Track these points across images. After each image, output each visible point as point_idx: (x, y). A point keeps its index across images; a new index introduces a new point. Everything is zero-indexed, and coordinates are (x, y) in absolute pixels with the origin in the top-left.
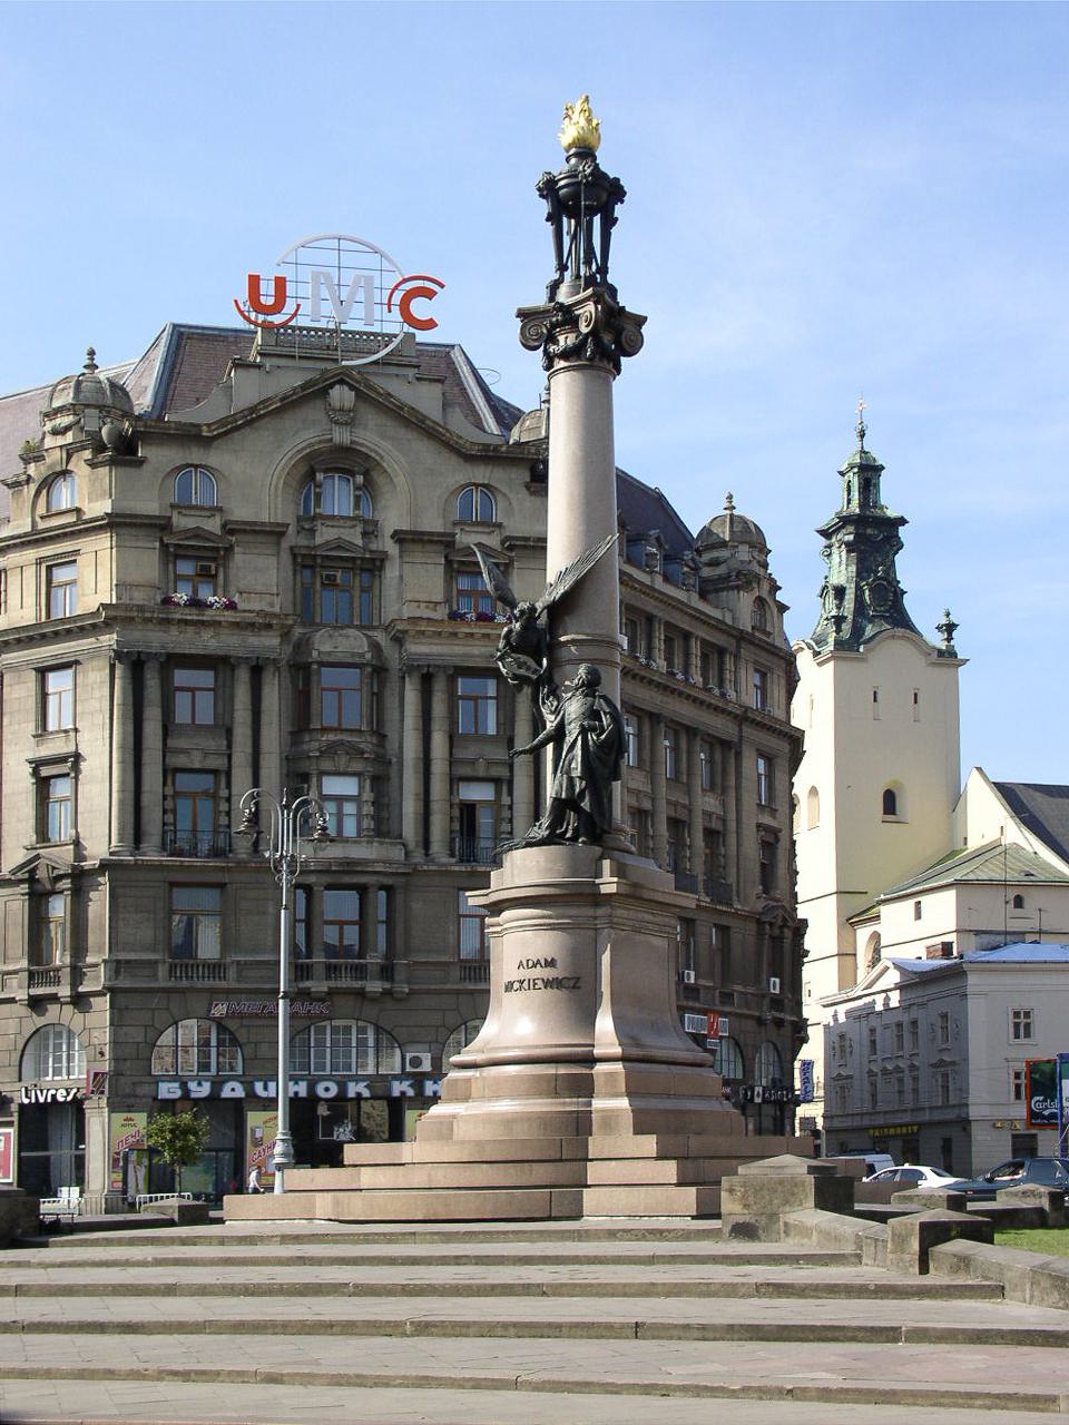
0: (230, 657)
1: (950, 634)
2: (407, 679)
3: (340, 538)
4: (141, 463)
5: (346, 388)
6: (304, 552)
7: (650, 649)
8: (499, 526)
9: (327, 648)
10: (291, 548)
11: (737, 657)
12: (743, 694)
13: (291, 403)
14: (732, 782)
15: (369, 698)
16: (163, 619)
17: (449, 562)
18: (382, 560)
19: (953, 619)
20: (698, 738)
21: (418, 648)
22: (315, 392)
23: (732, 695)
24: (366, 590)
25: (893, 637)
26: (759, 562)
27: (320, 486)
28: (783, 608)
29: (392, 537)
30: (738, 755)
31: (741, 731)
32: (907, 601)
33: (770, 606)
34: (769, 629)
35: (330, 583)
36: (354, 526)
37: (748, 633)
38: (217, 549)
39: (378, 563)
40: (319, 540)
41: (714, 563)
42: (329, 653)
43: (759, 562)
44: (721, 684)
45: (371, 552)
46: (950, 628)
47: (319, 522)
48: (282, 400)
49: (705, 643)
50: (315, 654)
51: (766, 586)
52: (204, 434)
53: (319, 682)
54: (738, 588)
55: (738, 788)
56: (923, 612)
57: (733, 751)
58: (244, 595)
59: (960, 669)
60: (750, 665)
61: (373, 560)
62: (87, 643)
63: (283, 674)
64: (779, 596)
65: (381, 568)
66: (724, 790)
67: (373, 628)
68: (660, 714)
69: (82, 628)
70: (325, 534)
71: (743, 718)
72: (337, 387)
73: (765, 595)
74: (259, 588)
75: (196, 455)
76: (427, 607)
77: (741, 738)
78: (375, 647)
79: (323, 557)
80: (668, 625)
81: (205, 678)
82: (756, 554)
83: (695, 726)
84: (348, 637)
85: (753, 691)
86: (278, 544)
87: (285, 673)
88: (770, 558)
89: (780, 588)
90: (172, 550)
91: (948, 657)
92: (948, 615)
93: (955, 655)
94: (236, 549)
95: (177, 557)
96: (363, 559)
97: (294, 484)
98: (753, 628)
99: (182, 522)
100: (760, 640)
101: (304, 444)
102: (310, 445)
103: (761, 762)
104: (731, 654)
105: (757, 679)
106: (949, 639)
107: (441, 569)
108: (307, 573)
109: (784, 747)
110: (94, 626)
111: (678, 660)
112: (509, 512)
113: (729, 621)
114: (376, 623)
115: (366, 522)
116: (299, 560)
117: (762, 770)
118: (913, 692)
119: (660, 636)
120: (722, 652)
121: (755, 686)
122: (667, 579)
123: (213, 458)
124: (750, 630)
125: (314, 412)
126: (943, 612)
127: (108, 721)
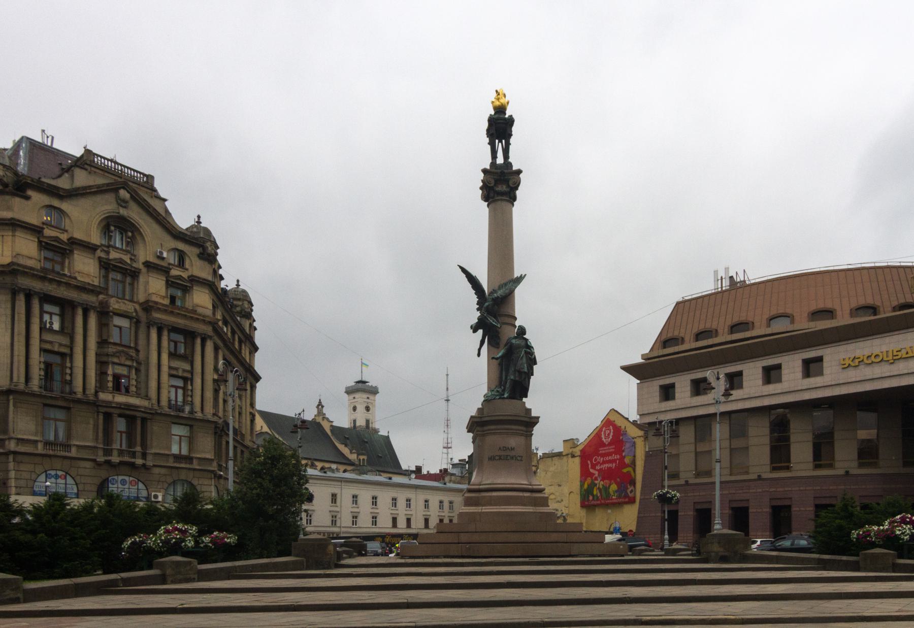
2: (151, 328)
8: (187, 269)
9: (116, 306)
16: (42, 276)
17: (167, 281)
21: (157, 315)
24: (132, 284)
42: (119, 309)
50: (111, 309)
53: (112, 321)
65: (138, 276)
76: (160, 298)
78: (136, 311)
81: (56, 309)
84: (124, 303)
107: (164, 282)
112: (192, 265)
114: (135, 300)
127: (9, 319)
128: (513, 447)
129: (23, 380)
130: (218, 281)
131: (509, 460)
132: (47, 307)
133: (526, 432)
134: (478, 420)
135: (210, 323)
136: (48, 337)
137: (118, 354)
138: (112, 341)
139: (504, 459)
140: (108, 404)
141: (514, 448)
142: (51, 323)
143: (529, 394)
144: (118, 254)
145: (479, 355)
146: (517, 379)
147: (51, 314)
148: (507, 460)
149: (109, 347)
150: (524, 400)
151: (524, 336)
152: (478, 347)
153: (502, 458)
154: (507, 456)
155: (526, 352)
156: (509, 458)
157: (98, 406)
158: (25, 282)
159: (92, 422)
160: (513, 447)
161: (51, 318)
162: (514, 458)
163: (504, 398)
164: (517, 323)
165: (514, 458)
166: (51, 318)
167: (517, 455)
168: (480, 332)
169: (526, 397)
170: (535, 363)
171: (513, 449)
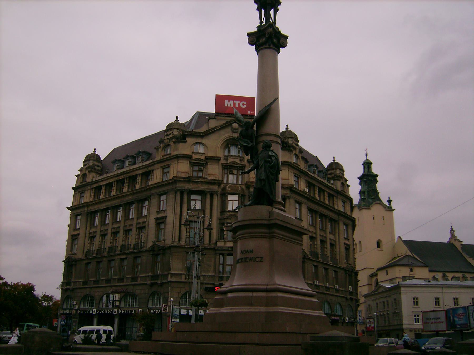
0: (205, 191)
1: (390, 202)
3: (234, 161)
4: (186, 142)
5: (236, 124)
6: (225, 165)
7: (314, 194)
10: (222, 163)
11: (337, 198)
12: (339, 207)
13: (222, 127)
14: (337, 231)
15: (240, 203)
18: (245, 167)
19: (391, 199)
20: (328, 218)
22: (228, 125)
23: (336, 208)
25: (377, 203)
26: (342, 174)
27: (229, 148)
28: (349, 186)
29: (247, 161)
30: (338, 224)
31: (339, 217)
32: (380, 195)
33: (345, 185)
34: (345, 191)
35: (232, 173)
36: (238, 158)
37: (339, 191)
38: (204, 163)
39: (244, 168)
40: (229, 162)
41: (330, 174)
43: (342, 174)
44: (333, 204)
45: (242, 165)
46: (389, 201)
47: (229, 157)
48: (220, 126)
49: (329, 193)
51: (344, 180)
52: (202, 135)
54: (337, 180)
55: (339, 233)
56: (384, 198)
57: (337, 223)
58: (209, 175)
59: (393, 211)
60: (341, 200)
61: (242, 167)
62: (170, 187)
63: (218, 196)
64: (348, 183)
66: (335, 232)
67: (242, 184)
68: (317, 211)
69: (169, 183)
70: (230, 160)
71: (339, 213)
72: (234, 123)
73: (344, 182)
74: (213, 174)
75: (199, 140)
77: (339, 219)
78: (242, 189)
79: (230, 166)
80: (319, 188)
81: (199, 197)
82: (341, 172)
83: (327, 215)
85: (342, 207)
86: (218, 162)
87: (219, 195)
88: (345, 173)
89: (347, 181)
90: (192, 163)
91: (390, 209)
92: (389, 198)
93: (391, 208)
94: (208, 164)
95: (194, 165)
96: (240, 167)
97: (223, 147)
98: (341, 190)
99: (195, 157)
100: (343, 193)
101: (226, 137)
102: (227, 138)
103: (345, 226)
104: (336, 197)
105: (342, 204)
106: (390, 204)
108: (226, 170)
109: (350, 223)
110: (172, 182)
111: (322, 197)
113: (335, 188)
115: (241, 157)
116: (224, 166)
117: (345, 228)
118: (382, 217)
119: (317, 190)
120: (333, 196)
121: (342, 206)
122: (318, 176)
123: (204, 141)
124: (340, 191)
125: (229, 130)
126: (388, 198)
127: (174, 207)
128: (251, 250)
129: (177, 239)
130: (300, 161)
131: (248, 262)
132: (193, 197)
133: (269, 233)
135: (287, 188)
136: (191, 213)
137: (230, 218)
138: (227, 210)
140: (221, 249)
142: (195, 205)
144: (232, 159)
147: (196, 200)
148: (246, 262)
149: (225, 214)
153: (243, 260)
154: (246, 258)
155: (266, 162)
156: (248, 260)
157: (216, 250)
158: (181, 186)
159: (213, 260)
160: (251, 250)
161: (196, 203)
162: (253, 260)
165: (253, 260)
166: (196, 203)
167: (255, 258)
171: (252, 251)
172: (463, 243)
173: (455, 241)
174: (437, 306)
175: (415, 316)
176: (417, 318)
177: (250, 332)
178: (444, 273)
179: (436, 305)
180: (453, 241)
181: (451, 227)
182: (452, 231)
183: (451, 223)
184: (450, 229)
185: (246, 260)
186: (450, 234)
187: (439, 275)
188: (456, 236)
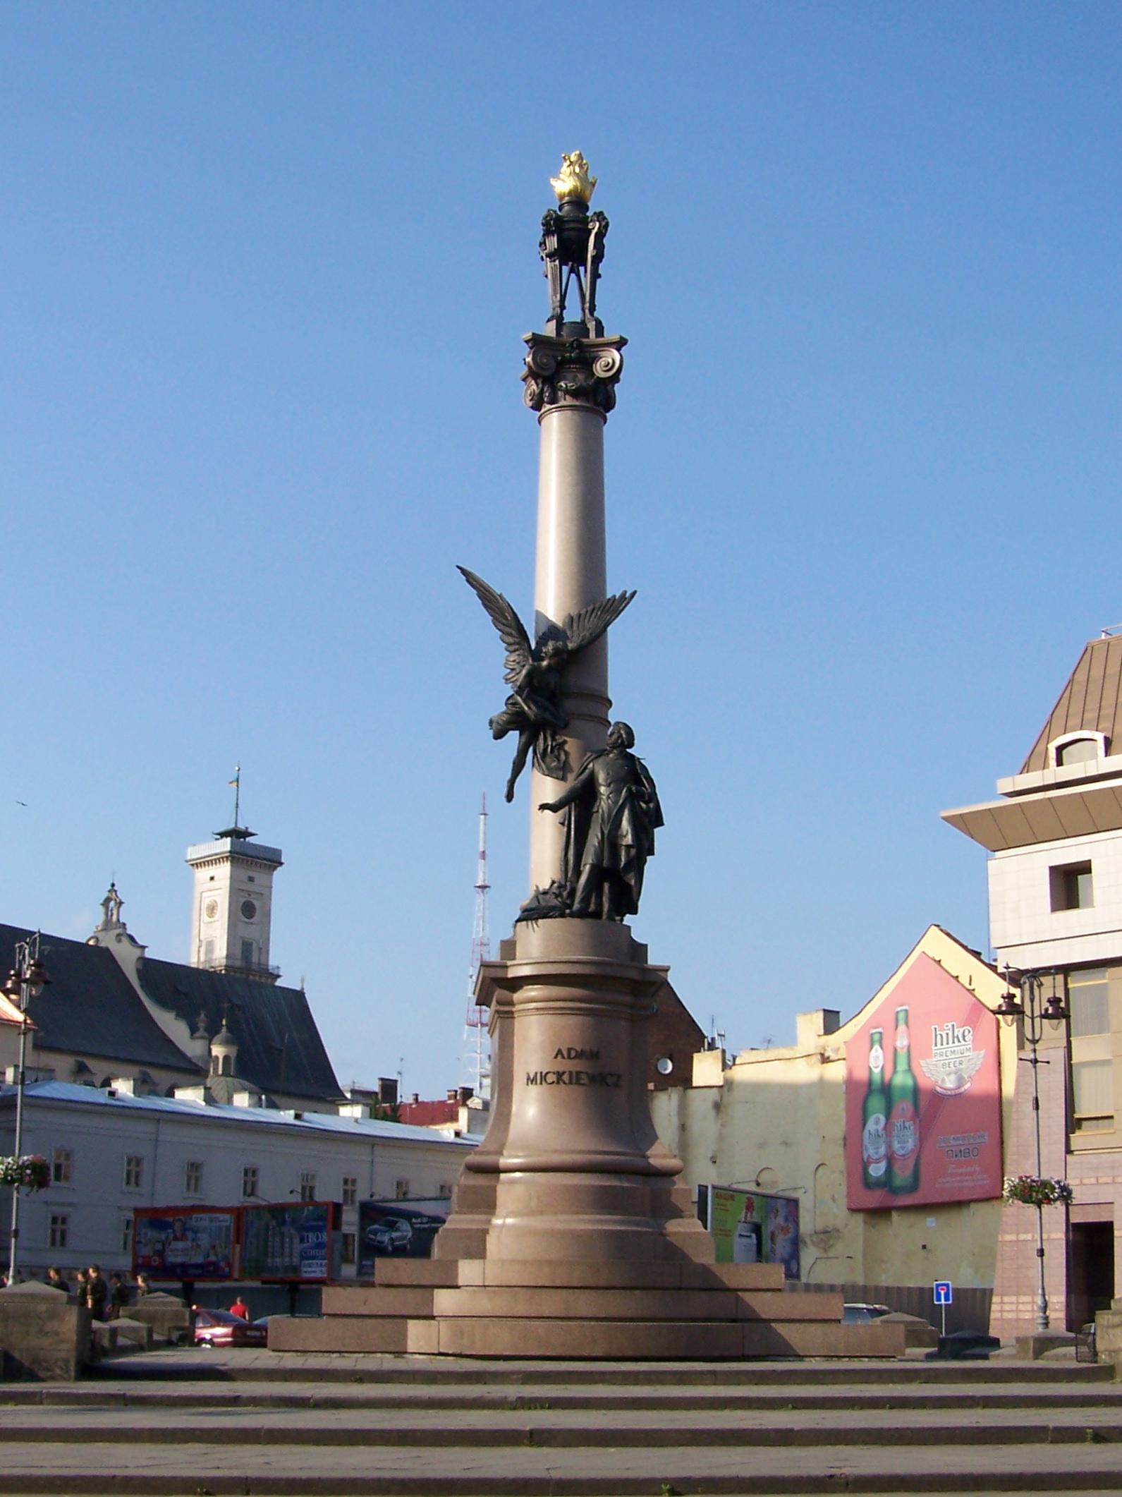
134: (499, 973)
139: (571, 1083)
141: (598, 1052)
143: (642, 904)
145: (510, 797)
146: (605, 863)
150: (628, 919)
151: (628, 750)
152: (509, 776)
154: (578, 1073)
163: (572, 915)
164: (613, 716)
168: (513, 737)
169: (634, 910)
170: (659, 822)
172: (149, 954)
173: (119, 941)
174: (132, 1188)
175: (55, 1220)
176: (59, 1226)
177: (680, 1289)
178: (79, 1059)
179: (128, 1183)
180: (108, 941)
181: (113, 885)
182: (111, 901)
183: (114, 873)
184: (106, 894)
185: (578, 1078)
186: (102, 909)
187: (63, 1063)
188: (124, 924)
